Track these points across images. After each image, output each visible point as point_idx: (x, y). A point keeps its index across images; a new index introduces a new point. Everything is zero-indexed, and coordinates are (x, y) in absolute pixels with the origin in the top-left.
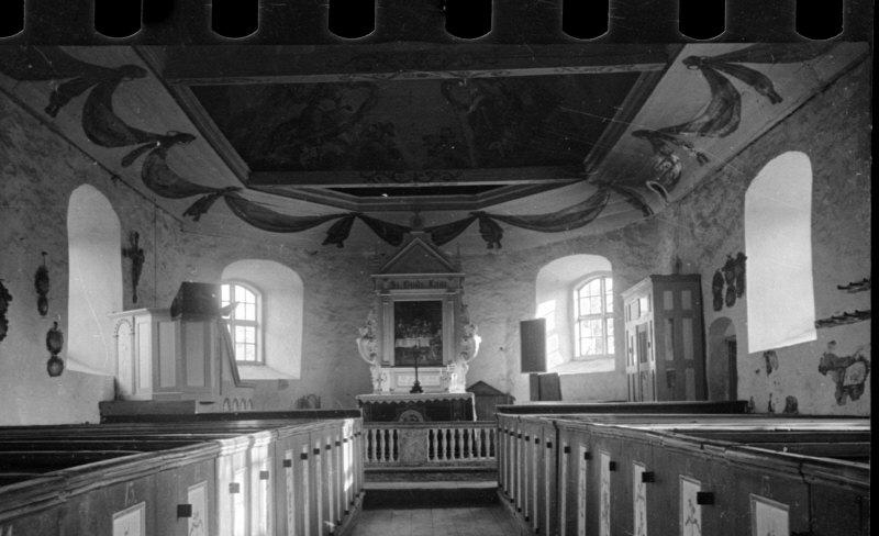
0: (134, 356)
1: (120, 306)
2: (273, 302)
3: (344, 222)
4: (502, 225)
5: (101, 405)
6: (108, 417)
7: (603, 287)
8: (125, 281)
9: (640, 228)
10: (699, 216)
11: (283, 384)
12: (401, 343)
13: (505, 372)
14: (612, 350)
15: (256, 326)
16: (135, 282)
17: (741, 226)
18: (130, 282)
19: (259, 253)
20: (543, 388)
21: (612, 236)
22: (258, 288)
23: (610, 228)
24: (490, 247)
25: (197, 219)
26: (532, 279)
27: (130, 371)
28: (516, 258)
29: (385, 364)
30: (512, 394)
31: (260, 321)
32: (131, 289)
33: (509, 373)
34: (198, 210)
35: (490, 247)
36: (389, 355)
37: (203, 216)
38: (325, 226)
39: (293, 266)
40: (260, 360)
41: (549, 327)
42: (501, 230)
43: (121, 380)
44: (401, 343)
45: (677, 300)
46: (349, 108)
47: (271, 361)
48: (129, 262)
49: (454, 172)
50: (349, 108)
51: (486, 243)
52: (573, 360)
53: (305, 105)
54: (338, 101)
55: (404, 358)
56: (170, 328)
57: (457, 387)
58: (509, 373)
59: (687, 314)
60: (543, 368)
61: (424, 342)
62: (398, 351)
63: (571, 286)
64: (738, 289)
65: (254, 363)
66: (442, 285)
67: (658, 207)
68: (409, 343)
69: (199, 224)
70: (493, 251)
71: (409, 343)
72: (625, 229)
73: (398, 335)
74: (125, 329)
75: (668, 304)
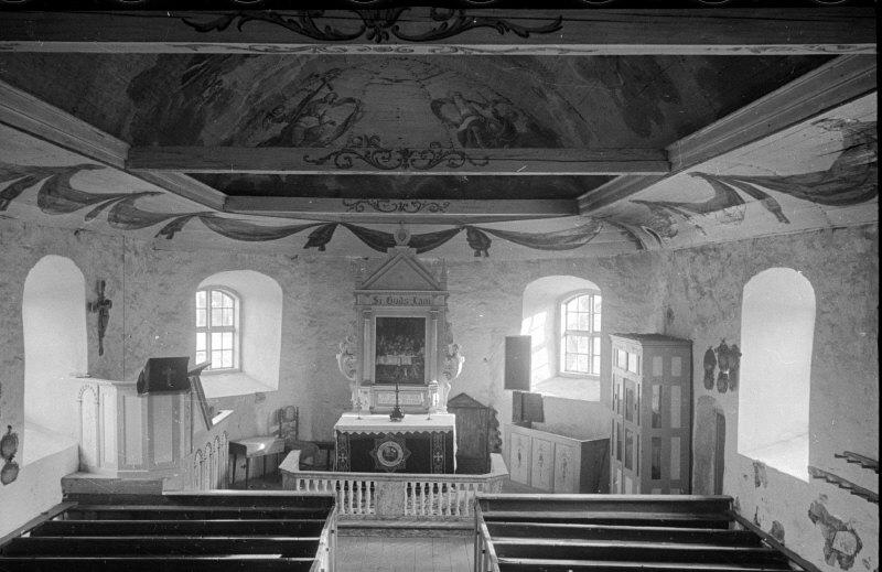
0: (98, 426)
1: (84, 370)
2: (251, 306)
3: (324, 229)
4: (489, 235)
5: (63, 481)
6: (71, 495)
7: (591, 305)
8: (90, 338)
9: (633, 259)
10: (695, 278)
11: (260, 397)
12: (382, 361)
13: (488, 384)
14: (597, 371)
15: (234, 332)
16: (101, 335)
17: (738, 316)
18: (96, 330)
19: (235, 264)
20: (526, 406)
21: (603, 262)
22: (236, 293)
23: (602, 254)
24: (478, 254)
25: (170, 237)
26: (520, 294)
27: (94, 441)
28: (503, 268)
29: (366, 383)
30: (496, 407)
31: (237, 326)
32: (97, 343)
33: (493, 385)
34: (170, 231)
35: (478, 254)
36: (370, 374)
37: (176, 234)
38: (305, 235)
39: (273, 273)
40: (237, 367)
41: (534, 344)
42: (489, 241)
43: (84, 447)
44: (382, 361)
45: (667, 368)
46: (333, 123)
47: (248, 368)
48: (95, 316)
49: (441, 203)
50: (333, 123)
51: (474, 251)
52: (558, 375)
53: (284, 124)
54: (320, 118)
55: (385, 376)
56: (137, 403)
57: (442, 419)
58: (493, 385)
59: (677, 381)
60: (528, 389)
61: (406, 359)
62: (379, 367)
63: (559, 300)
64: (730, 381)
65: (231, 371)
66: (428, 302)
67: (651, 245)
68: (391, 360)
69: (172, 241)
70: (480, 259)
71: (391, 360)
72: (618, 257)
73: (380, 352)
74: (89, 396)
75: (658, 371)
